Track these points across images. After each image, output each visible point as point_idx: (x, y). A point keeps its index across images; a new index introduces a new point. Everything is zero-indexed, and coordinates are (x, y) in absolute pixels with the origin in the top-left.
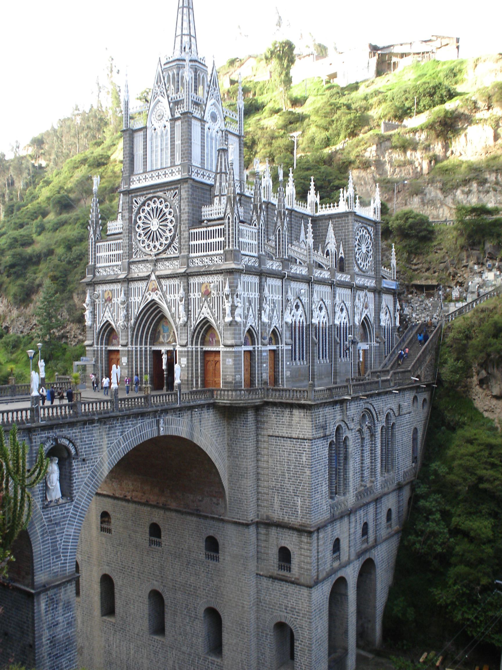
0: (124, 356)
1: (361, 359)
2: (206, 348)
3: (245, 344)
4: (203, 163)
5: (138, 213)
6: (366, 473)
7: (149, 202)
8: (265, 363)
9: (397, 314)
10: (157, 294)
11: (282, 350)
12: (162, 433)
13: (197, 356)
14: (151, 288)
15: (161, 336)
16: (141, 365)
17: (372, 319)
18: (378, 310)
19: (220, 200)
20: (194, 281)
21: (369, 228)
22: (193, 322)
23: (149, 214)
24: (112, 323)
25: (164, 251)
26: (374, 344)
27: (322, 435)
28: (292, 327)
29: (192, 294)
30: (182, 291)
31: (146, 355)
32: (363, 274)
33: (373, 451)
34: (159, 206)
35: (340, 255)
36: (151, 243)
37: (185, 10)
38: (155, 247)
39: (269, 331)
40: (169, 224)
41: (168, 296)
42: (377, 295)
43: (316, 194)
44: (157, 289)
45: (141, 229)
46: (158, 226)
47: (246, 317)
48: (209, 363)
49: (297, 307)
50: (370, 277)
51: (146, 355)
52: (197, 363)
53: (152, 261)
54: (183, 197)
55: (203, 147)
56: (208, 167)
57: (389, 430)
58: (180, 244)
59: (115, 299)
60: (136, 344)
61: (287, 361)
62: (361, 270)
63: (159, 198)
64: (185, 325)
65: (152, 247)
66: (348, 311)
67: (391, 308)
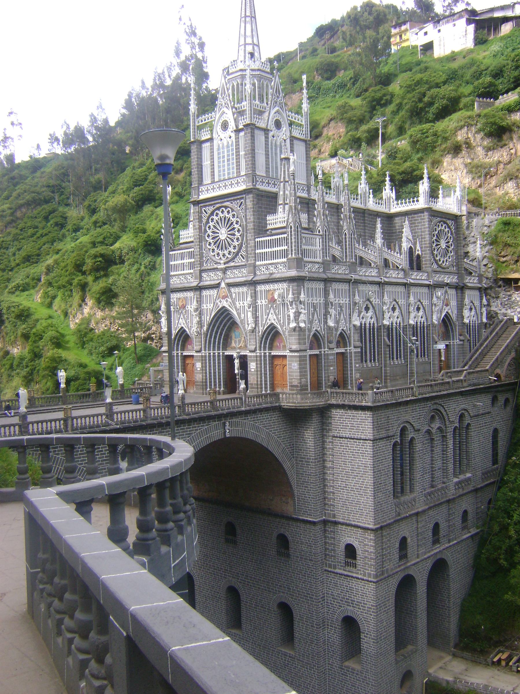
0: (199, 361)
1: (443, 359)
2: (274, 353)
3: (311, 348)
4: (267, 171)
5: (207, 222)
6: (438, 474)
7: (217, 211)
8: (331, 366)
9: (484, 309)
10: (227, 301)
11: (351, 353)
12: (228, 435)
13: (265, 360)
14: (221, 296)
15: (233, 342)
16: (214, 370)
18: (460, 307)
19: (284, 209)
20: (260, 288)
21: (449, 222)
22: (261, 328)
23: (218, 223)
24: (187, 330)
25: (232, 260)
26: (457, 341)
27: (384, 435)
28: (361, 330)
29: (259, 301)
30: (249, 299)
31: (219, 360)
33: (444, 451)
34: (227, 215)
35: (417, 253)
36: (220, 252)
37: (248, 19)
38: (224, 255)
39: (336, 334)
40: (236, 233)
41: (237, 303)
42: (459, 292)
43: (392, 190)
44: (227, 297)
45: (211, 238)
46: (226, 235)
47: (311, 322)
48: (278, 367)
49: (367, 309)
50: (450, 273)
51: (219, 360)
52: (265, 367)
53: (221, 269)
54: (248, 207)
55: (267, 155)
56: (273, 175)
57: (462, 432)
58: (247, 253)
59: (189, 307)
60: (209, 350)
61: (356, 363)
62: (439, 266)
63: (226, 207)
64: (253, 331)
65: (221, 256)
66: (425, 310)
67: (477, 303)
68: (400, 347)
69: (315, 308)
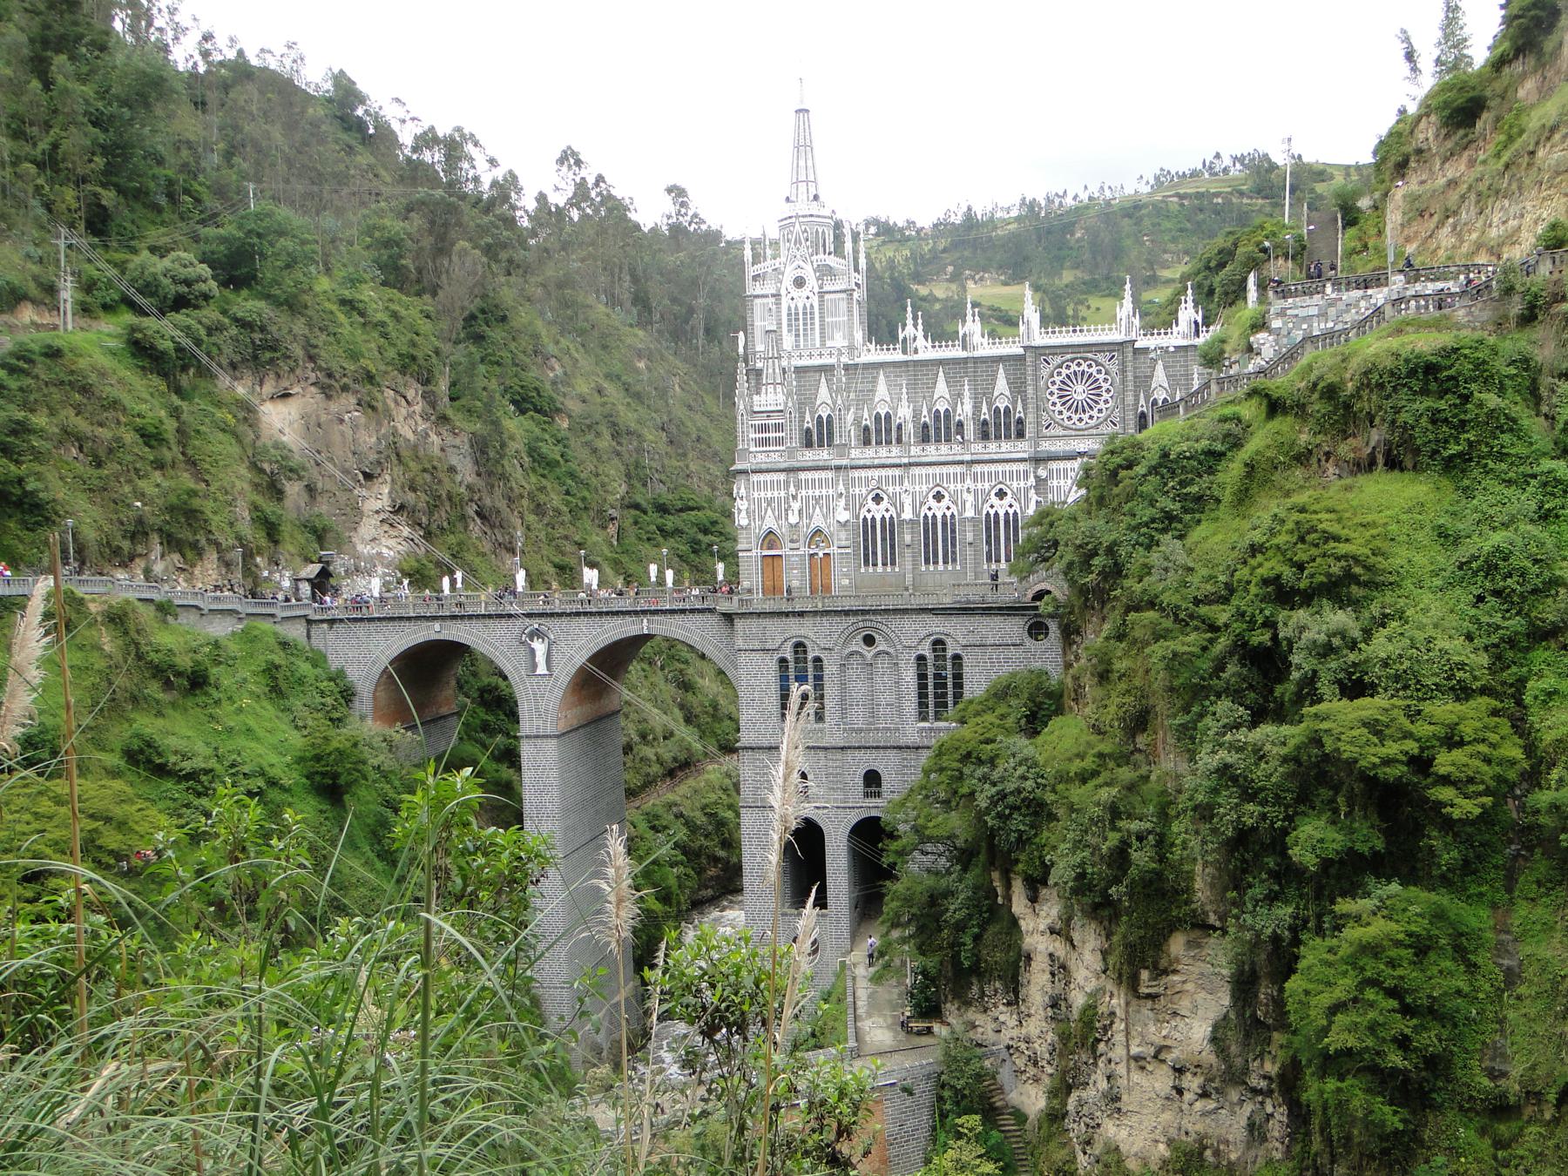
21: (1100, 357)
32: (1080, 434)
47: (762, 519)
68: (954, 545)
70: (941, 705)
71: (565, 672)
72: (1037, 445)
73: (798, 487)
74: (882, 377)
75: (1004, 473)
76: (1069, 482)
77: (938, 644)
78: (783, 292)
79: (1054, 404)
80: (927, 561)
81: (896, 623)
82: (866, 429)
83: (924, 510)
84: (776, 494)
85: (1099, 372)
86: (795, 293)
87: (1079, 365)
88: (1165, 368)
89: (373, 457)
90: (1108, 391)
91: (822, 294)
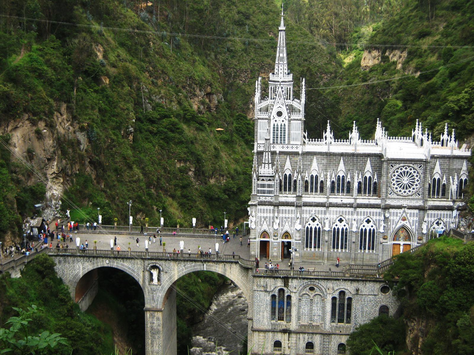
12: (205, 269)
17: (413, 228)
18: (420, 223)
21: (415, 166)
32: (405, 198)
47: (261, 225)
68: (346, 241)
69: (265, 220)
70: (341, 315)
71: (166, 284)
72: (386, 201)
73: (278, 213)
74: (315, 160)
75: (370, 213)
76: (398, 218)
77: (342, 293)
78: (272, 117)
79: (394, 184)
80: (334, 248)
81: (323, 284)
82: (307, 181)
83: (334, 226)
84: (268, 215)
85: (414, 172)
86: (277, 118)
87: (406, 168)
88: (440, 165)
89: (52, 150)
90: (418, 181)
91: (289, 121)
